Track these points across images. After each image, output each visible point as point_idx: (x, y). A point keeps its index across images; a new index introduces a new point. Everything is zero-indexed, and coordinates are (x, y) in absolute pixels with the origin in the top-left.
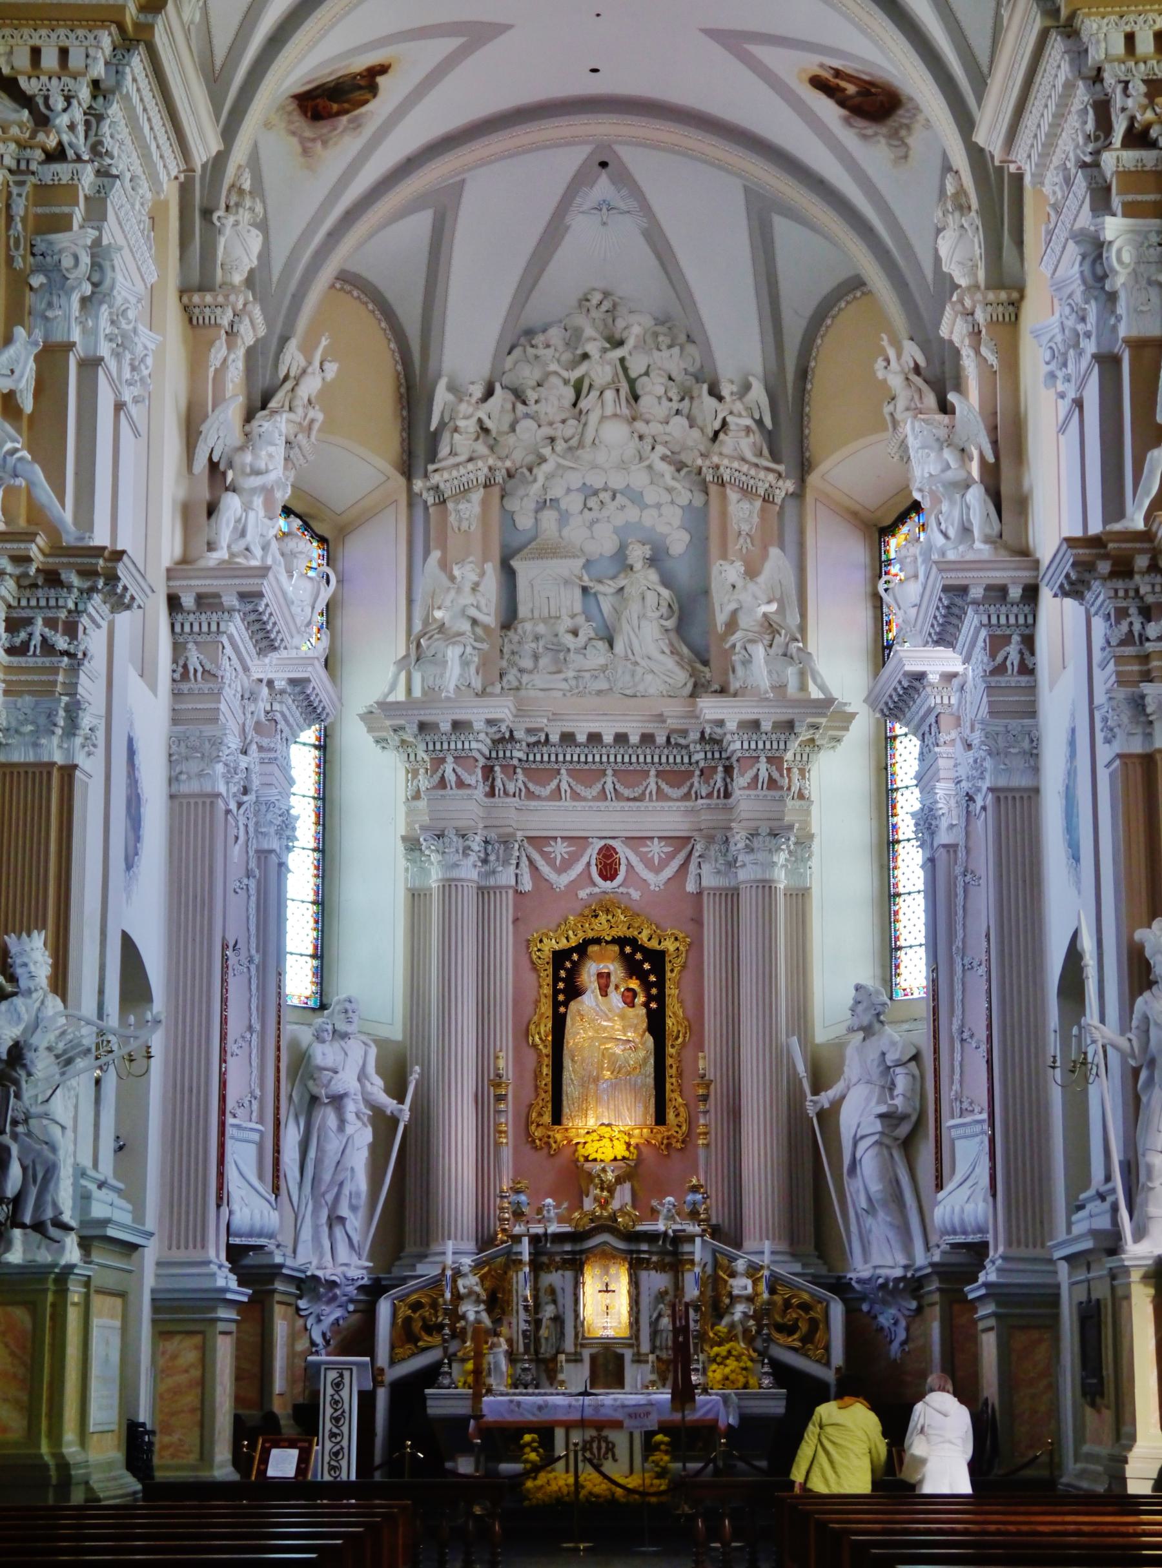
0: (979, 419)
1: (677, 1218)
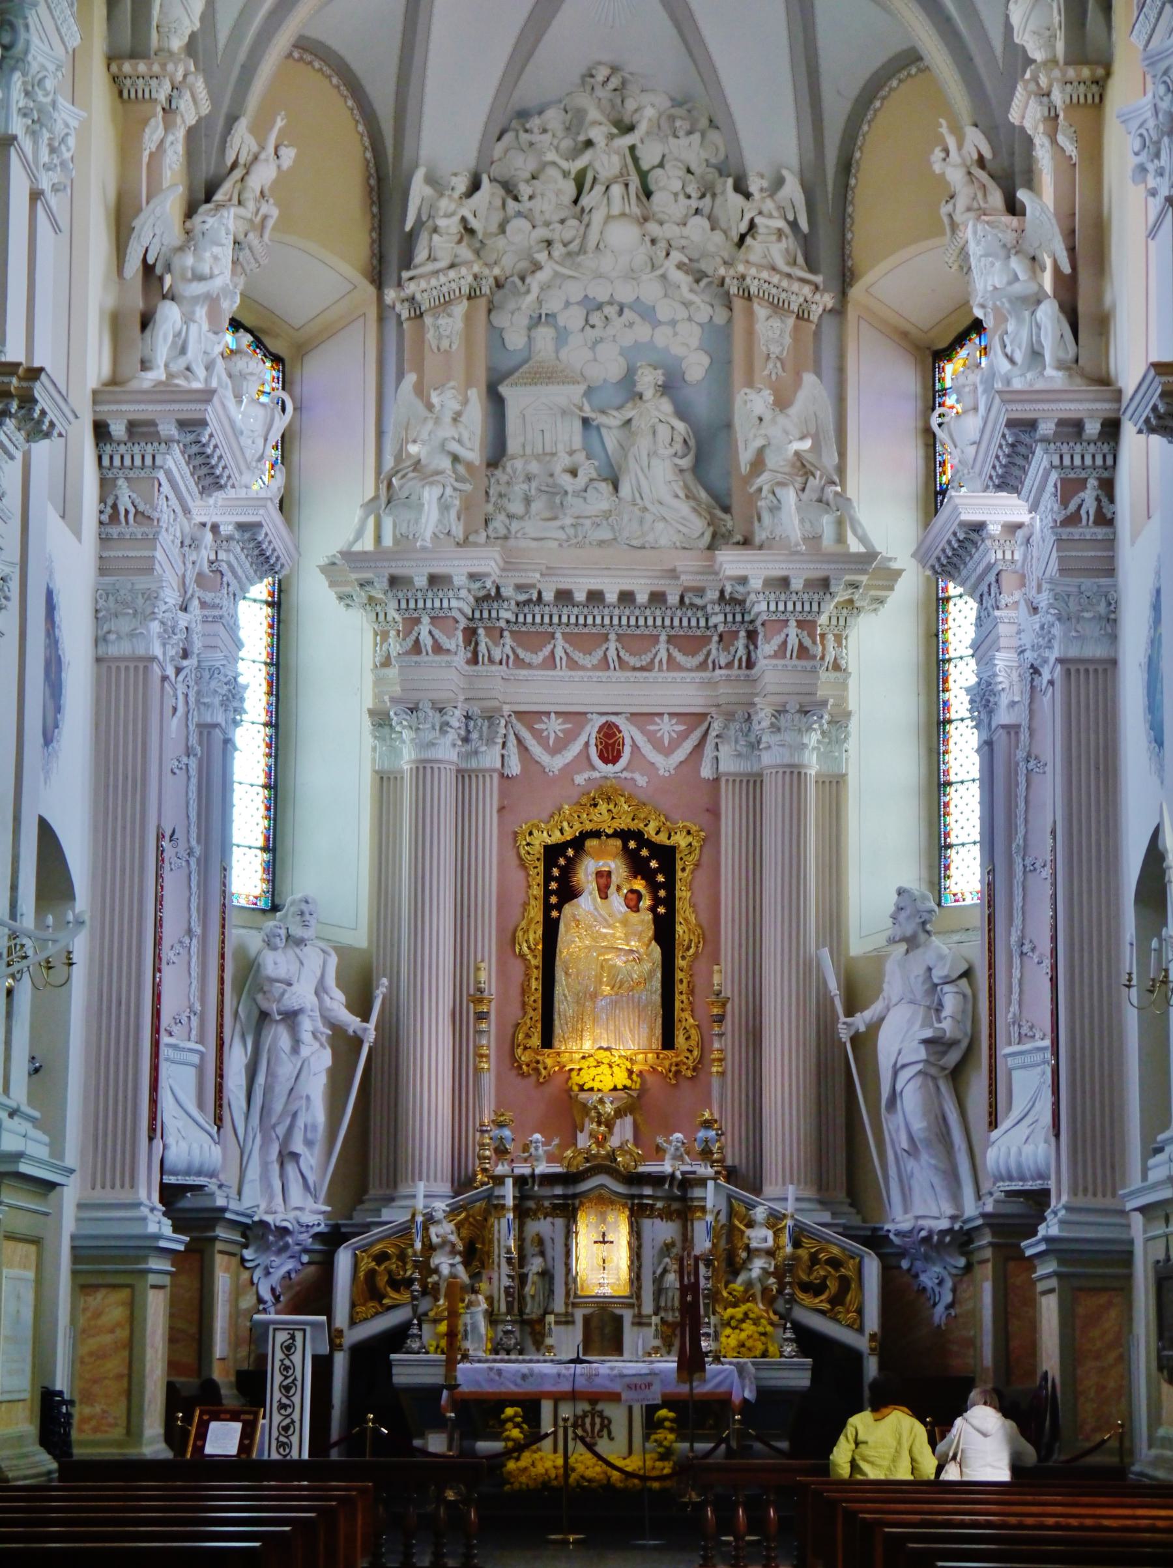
0: (1054, 221)
1: (686, 1157)
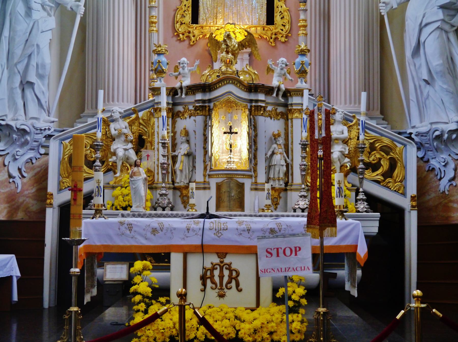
1: (288, 75)
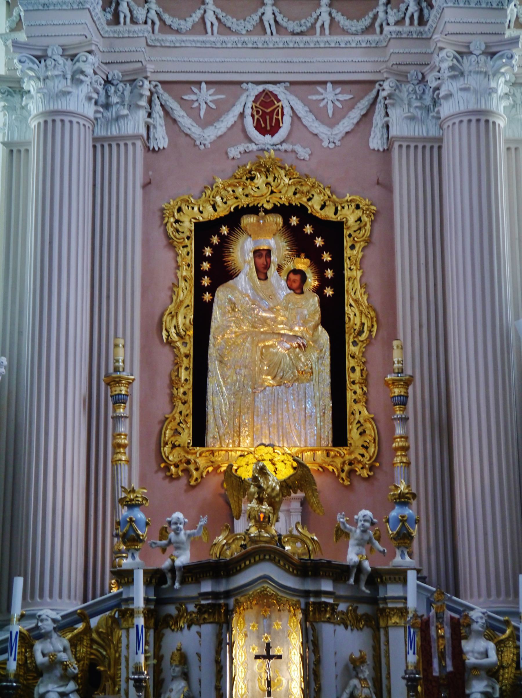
1: (377, 543)
